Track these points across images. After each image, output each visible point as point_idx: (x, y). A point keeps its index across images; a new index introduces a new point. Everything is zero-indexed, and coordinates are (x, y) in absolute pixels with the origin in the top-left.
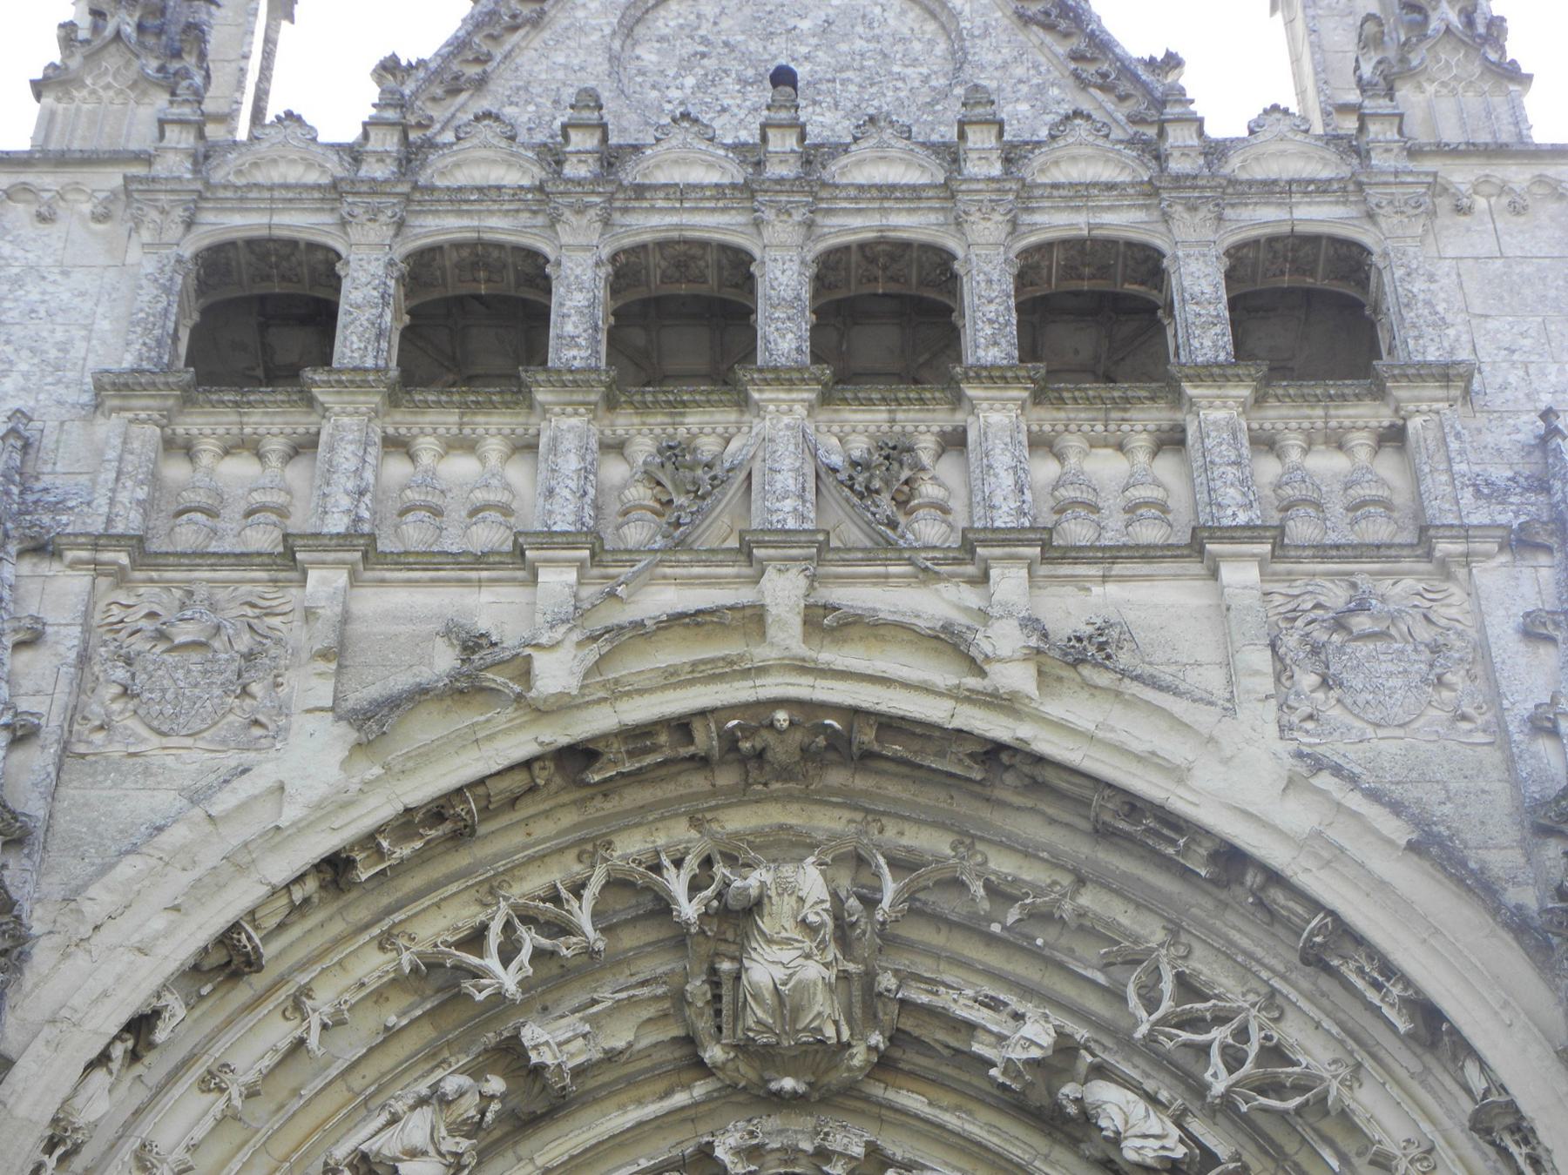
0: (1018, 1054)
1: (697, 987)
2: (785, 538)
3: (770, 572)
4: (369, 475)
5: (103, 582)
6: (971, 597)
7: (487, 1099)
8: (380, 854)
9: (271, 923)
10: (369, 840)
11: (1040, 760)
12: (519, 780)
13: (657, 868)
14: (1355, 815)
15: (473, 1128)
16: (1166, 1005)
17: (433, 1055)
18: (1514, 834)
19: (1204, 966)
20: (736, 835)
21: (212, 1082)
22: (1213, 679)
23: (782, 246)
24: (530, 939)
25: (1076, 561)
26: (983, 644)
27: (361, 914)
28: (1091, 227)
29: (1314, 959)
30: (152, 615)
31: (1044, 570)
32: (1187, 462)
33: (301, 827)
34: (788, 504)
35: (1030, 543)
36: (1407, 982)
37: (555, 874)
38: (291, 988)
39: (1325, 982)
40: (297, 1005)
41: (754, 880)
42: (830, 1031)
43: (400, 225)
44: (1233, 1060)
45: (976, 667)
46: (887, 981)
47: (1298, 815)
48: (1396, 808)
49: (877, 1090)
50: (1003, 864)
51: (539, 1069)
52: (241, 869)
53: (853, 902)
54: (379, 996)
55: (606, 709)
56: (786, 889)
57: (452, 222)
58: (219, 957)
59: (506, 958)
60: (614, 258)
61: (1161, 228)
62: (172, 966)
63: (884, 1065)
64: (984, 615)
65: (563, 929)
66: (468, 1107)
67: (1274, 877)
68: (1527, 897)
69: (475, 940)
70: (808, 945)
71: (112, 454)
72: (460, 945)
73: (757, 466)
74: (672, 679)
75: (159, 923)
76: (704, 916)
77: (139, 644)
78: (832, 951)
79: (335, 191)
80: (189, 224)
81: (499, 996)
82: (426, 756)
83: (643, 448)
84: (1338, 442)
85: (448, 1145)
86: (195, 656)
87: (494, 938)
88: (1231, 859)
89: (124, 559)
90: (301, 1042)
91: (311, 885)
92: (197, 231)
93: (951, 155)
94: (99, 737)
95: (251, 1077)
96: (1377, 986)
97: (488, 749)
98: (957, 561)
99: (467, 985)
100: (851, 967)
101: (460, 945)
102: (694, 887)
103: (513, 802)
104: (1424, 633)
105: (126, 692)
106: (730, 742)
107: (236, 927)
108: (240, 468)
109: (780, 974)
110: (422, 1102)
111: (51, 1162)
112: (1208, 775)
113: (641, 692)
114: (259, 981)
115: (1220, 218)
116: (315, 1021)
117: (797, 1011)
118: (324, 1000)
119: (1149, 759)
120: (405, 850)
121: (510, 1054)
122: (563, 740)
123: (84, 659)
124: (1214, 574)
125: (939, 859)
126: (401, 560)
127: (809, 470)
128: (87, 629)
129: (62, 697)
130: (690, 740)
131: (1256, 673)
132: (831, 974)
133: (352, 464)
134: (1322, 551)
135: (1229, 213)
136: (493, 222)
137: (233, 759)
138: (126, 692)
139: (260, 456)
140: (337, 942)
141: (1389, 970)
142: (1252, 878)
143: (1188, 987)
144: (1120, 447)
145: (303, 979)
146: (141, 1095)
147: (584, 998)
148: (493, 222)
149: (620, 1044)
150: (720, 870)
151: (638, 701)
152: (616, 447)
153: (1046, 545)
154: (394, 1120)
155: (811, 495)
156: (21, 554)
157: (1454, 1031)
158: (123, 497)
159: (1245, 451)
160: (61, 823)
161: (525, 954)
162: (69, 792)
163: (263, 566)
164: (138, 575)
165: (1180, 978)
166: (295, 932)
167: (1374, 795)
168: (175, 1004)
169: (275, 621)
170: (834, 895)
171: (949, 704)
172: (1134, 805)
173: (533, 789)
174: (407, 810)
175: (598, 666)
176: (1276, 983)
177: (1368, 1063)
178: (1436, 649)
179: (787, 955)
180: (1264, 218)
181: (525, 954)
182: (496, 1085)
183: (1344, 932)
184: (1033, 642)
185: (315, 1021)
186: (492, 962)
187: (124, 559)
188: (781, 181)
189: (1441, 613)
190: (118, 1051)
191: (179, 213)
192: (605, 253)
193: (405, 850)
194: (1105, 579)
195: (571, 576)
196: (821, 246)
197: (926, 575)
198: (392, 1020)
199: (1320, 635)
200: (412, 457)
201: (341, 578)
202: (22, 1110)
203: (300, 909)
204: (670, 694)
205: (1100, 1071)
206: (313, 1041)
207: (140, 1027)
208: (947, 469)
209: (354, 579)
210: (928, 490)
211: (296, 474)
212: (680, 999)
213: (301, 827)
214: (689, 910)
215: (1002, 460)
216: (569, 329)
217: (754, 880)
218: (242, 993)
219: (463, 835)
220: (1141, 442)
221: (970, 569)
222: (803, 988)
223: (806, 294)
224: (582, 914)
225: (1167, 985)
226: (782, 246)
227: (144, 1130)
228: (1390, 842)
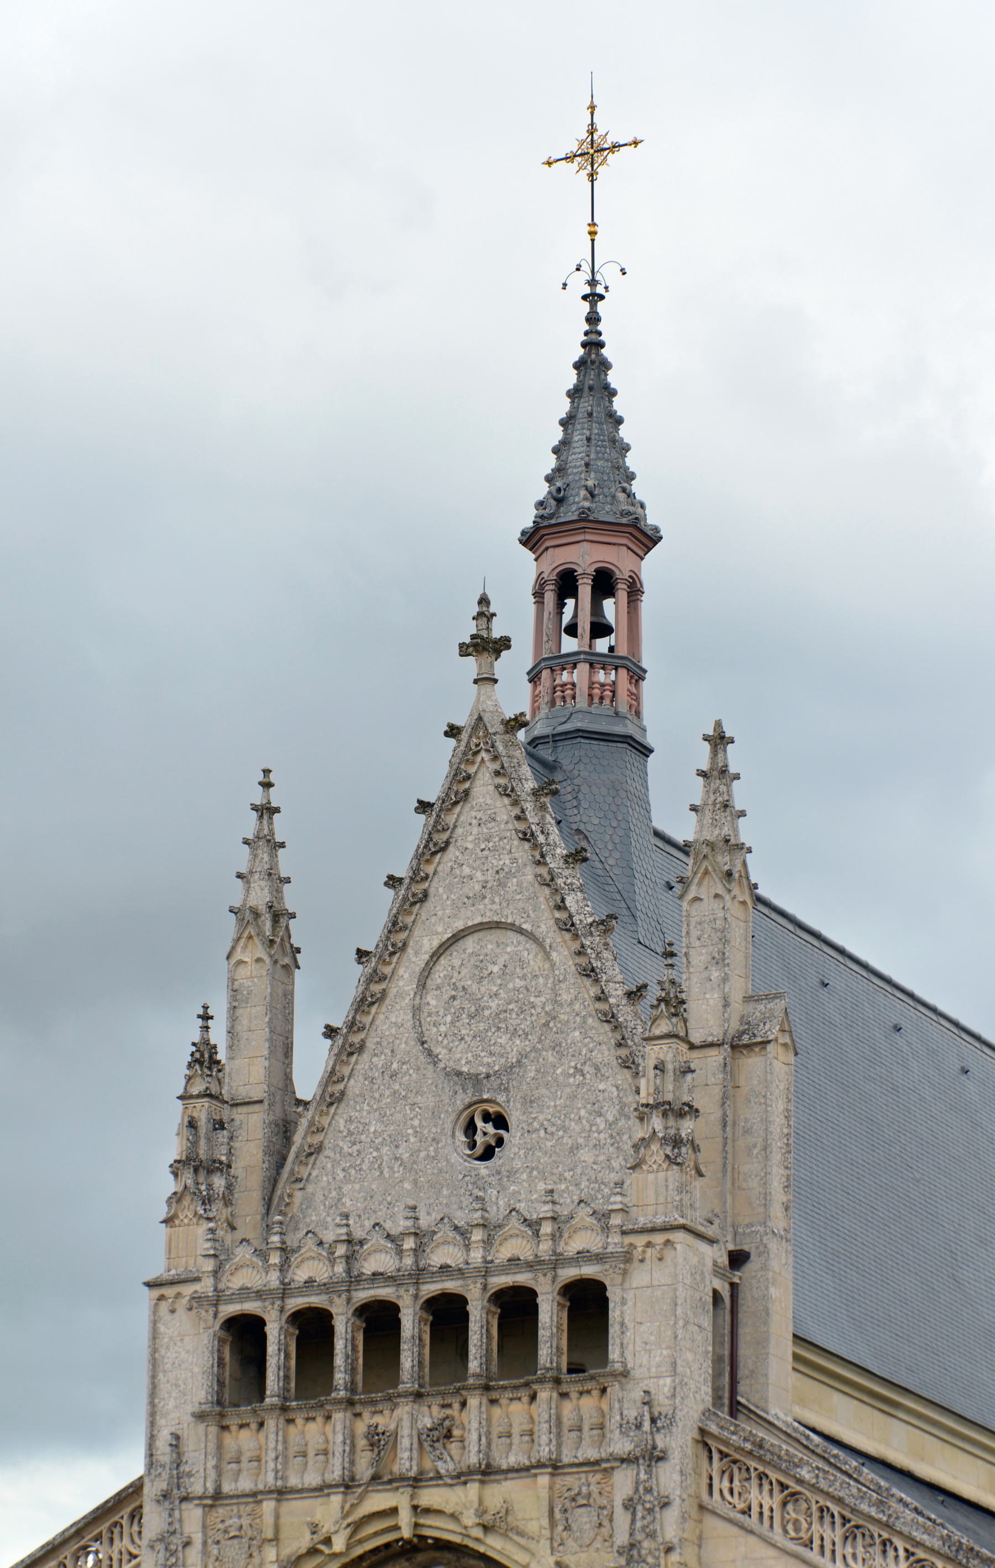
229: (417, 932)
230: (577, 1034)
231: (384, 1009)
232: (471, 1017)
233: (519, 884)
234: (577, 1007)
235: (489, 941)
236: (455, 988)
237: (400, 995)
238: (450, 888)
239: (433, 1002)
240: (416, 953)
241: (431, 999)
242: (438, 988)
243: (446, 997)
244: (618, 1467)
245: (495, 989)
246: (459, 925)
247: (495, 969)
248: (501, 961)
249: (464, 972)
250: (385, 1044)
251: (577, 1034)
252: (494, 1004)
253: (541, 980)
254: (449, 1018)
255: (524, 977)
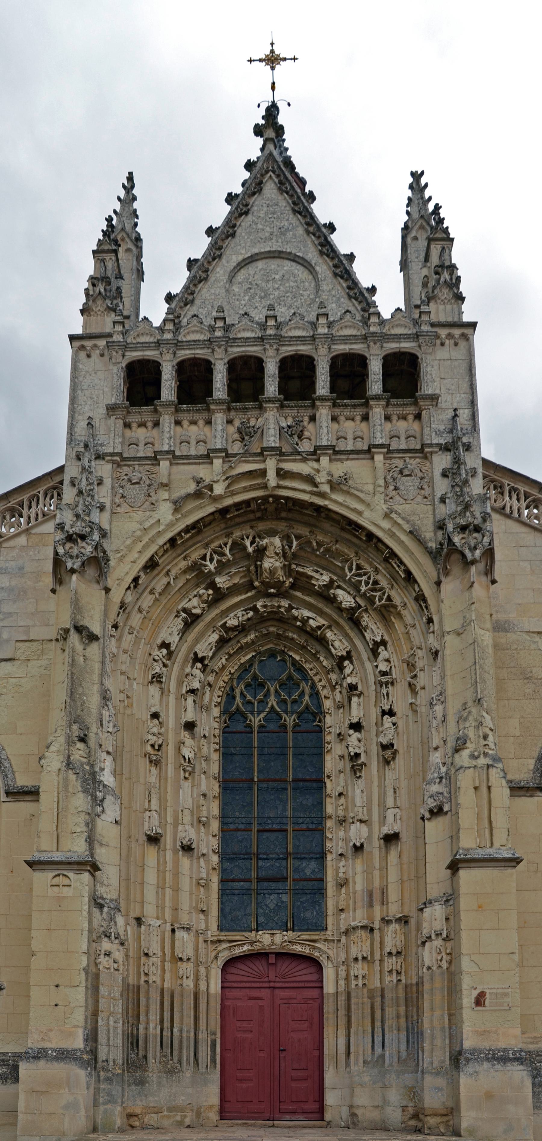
0: (321, 583)
1: (252, 568)
2: (272, 449)
3: (268, 459)
4: (172, 432)
5: (115, 466)
6: (315, 465)
7: (209, 595)
8: (182, 537)
9: (160, 554)
10: (179, 534)
11: (330, 510)
12: (211, 517)
13: (243, 539)
14: (399, 524)
15: (206, 602)
16: (354, 571)
17: (197, 586)
18: (432, 528)
19: (362, 563)
20: (261, 531)
21: (151, 592)
22: (370, 488)
23: (271, 357)
24: (216, 557)
25: (341, 454)
26: (318, 480)
27: (179, 551)
28: (350, 349)
29: (386, 560)
30: (126, 475)
31: (333, 457)
32: (369, 424)
33: (164, 531)
34: (272, 439)
35: (330, 449)
36: (405, 565)
37: (221, 542)
38: (166, 570)
39: (388, 565)
40: (167, 574)
41: (265, 542)
42: (281, 578)
43: (175, 354)
44: (367, 584)
45: (316, 485)
46: (294, 566)
47: (386, 525)
48: (408, 522)
49: (291, 591)
50: (320, 538)
51: (220, 588)
52: (153, 542)
53: (287, 547)
54: (185, 572)
55: (230, 498)
56: (272, 544)
57: (188, 352)
58: (150, 564)
59: (211, 560)
60: (228, 362)
61: (367, 350)
62: (140, 566)
63: (293, 586)
64: (318, 471)
65: (224, 555)
66: (205, 597)
67: (379, 540)
68: (432, 545)
69: (204, 558)
70: (277, 558)
71: (112, 429)
72: (201, 559)
73: (265, 427)
74: (246, 490)
75: (136, 555)
76: (254, 551)
77: (124, 483)
78: (282, 559)
79: (158, 344)
80: (123, 356)
81: (210, 571)
82: (190, 512)
83: (237, 423)
84: (405, 418)
85: (202, 605)
86: (137, 486)
87: (208, 557)
88: (370, 536)
89: (118, 459)
90: (169, 583)
91: (168, 545)
92: (126, 357)
93: (314, 325)
94: (118, 508)
95: (160, 591)
96: (399, 566)
97: (204, 510)
98: (312, 455)
99: (203, 568)
100: (286, 563)
101: (201, 559)
102: (252, 543)
103: (210, 524)
104: (420, 474)
105: (123, 496)
106: (259, 505)
107: (153, 556)
108: (142, 431)
109: (270, 565)
110: (195, 596)
111: (121, 611)
112: (367, 514)
113: (238, 493)
114: (159, 568)
115: (382, 347)
116: (172, 577)
117: (274, 574)
118: (173, 573)
119: (355, 510)
120: (187, 536)
121: (212, 585)
122: (221, 507)
123: (113, 488)
124: (372, 458)
125: (306, 536)
126: (182, 457)
127: (277, 428)
128: (112, 479)
129: (109, 499)
130: (250, 506)
131: (380, 486)
132: (282, 565)
133: (167, 429)
134: (399, 451)
135: (385, 345)
136: (198, 351)
137: (148, 513)
138: (123, 496)
139: (146, 428)
140: (175, 558)
141: (402, 563)
142: (375, 540)
143: (359, 567)
144: (353, 420)
145: (168, 567)
146: (138, 595)
147: (228, 571)
148: (198, 351)
149: (236, 582)
150: (257, 539)
151: (238, 496)
152: (230, 422)
153: (334, 450)
154: (190, 600)
155: (278, 436)
156: (96, 459)
157: (414, 577)
158: (116, 441)
159: (383, 421)
160: (113, 531)
161: (215, 561)
162: (114, 524)
163: (150, 460)
164: (122, 463)
165: (357, 565)
166: (166, 556)
167: (403, 519)
168: (142, 574)
169: (154, 476)
170: (282, 545)
171: (309, 495)
172: (351, 522)
173: (214, 519)
174: (187, 526)
175: (228, 487)
176: (378, 566)
177: (395, 585)
178: (422, 478)
179: (272, 560)
180: (392, 346)
181: (215, 561)
182: (211, 592)
183: (393, 555)
184: (330, 478)
185: (172, 577)
186: (208, 563)
187: (118, 459)
188: (270, 335)
189: (424, 469)
190: (132, 586)
191: (120, 352)
192: (226, 361)
193: (187, 536)
194: (347, 459)
195: (221, 461)
196: (281, 357)
197: (304, 460)
198: (188, 577)
199: (396, 475)
200: (182, 426)
201: (167, 463)
202: (114, 600)
203: (166, 551)
204: (245, 494)
205: (339, 587)
206: (172, 582)
207: (136, 580)
208: (311, 427)
209: (171, 464)
210: (306, 434)
211: (155, 432)
212: (248, 570)
213: (164, 531)
214: (250, 549)
215: (325, 424)
216: (218, 386)
217: (265, 542)
218: (156, 572)
219: (200, 532)
220: (358, 418)
221: (315, 457)
222: (276, 568)
223: (277, 373)
224: (227, 551)
225: (354, 567)
226: (271, 357)
227: (139, 603)
228: (405, 531)
229: (228, 252)
230: (334, 305)
231: (207, 286)
232: (261, 298)
233: (294, 235)
234: (333, 293)
235: (273, 264)
236: (251, 283)
237: (217, 281)
238: (249, 233)
239: (236, 290)
240: (228, 262)
241: (236, 289)
242: (240, 283)
243: (245, 288)
244: (436, 452)
245: (277, 286)
246: (256, 250)
247: (277, 277)
248: (281, 274)
249: (256, 277)
250: (207, 303)
251: (334, 305)
252: (276, 293)
253: (307, 284)
254: (247, 298)
255: (296, 281)
